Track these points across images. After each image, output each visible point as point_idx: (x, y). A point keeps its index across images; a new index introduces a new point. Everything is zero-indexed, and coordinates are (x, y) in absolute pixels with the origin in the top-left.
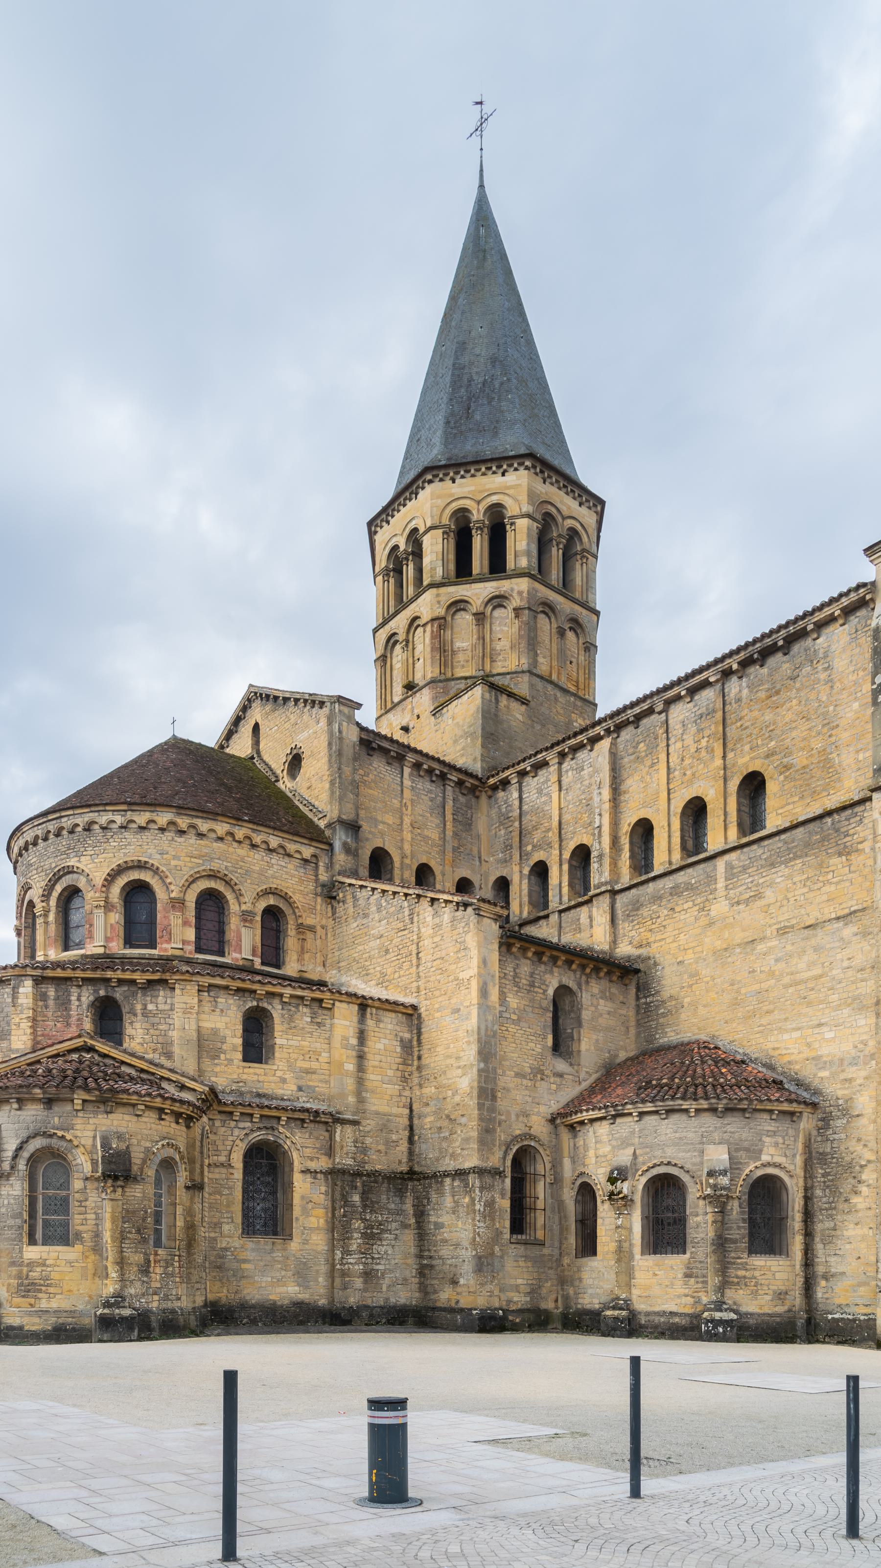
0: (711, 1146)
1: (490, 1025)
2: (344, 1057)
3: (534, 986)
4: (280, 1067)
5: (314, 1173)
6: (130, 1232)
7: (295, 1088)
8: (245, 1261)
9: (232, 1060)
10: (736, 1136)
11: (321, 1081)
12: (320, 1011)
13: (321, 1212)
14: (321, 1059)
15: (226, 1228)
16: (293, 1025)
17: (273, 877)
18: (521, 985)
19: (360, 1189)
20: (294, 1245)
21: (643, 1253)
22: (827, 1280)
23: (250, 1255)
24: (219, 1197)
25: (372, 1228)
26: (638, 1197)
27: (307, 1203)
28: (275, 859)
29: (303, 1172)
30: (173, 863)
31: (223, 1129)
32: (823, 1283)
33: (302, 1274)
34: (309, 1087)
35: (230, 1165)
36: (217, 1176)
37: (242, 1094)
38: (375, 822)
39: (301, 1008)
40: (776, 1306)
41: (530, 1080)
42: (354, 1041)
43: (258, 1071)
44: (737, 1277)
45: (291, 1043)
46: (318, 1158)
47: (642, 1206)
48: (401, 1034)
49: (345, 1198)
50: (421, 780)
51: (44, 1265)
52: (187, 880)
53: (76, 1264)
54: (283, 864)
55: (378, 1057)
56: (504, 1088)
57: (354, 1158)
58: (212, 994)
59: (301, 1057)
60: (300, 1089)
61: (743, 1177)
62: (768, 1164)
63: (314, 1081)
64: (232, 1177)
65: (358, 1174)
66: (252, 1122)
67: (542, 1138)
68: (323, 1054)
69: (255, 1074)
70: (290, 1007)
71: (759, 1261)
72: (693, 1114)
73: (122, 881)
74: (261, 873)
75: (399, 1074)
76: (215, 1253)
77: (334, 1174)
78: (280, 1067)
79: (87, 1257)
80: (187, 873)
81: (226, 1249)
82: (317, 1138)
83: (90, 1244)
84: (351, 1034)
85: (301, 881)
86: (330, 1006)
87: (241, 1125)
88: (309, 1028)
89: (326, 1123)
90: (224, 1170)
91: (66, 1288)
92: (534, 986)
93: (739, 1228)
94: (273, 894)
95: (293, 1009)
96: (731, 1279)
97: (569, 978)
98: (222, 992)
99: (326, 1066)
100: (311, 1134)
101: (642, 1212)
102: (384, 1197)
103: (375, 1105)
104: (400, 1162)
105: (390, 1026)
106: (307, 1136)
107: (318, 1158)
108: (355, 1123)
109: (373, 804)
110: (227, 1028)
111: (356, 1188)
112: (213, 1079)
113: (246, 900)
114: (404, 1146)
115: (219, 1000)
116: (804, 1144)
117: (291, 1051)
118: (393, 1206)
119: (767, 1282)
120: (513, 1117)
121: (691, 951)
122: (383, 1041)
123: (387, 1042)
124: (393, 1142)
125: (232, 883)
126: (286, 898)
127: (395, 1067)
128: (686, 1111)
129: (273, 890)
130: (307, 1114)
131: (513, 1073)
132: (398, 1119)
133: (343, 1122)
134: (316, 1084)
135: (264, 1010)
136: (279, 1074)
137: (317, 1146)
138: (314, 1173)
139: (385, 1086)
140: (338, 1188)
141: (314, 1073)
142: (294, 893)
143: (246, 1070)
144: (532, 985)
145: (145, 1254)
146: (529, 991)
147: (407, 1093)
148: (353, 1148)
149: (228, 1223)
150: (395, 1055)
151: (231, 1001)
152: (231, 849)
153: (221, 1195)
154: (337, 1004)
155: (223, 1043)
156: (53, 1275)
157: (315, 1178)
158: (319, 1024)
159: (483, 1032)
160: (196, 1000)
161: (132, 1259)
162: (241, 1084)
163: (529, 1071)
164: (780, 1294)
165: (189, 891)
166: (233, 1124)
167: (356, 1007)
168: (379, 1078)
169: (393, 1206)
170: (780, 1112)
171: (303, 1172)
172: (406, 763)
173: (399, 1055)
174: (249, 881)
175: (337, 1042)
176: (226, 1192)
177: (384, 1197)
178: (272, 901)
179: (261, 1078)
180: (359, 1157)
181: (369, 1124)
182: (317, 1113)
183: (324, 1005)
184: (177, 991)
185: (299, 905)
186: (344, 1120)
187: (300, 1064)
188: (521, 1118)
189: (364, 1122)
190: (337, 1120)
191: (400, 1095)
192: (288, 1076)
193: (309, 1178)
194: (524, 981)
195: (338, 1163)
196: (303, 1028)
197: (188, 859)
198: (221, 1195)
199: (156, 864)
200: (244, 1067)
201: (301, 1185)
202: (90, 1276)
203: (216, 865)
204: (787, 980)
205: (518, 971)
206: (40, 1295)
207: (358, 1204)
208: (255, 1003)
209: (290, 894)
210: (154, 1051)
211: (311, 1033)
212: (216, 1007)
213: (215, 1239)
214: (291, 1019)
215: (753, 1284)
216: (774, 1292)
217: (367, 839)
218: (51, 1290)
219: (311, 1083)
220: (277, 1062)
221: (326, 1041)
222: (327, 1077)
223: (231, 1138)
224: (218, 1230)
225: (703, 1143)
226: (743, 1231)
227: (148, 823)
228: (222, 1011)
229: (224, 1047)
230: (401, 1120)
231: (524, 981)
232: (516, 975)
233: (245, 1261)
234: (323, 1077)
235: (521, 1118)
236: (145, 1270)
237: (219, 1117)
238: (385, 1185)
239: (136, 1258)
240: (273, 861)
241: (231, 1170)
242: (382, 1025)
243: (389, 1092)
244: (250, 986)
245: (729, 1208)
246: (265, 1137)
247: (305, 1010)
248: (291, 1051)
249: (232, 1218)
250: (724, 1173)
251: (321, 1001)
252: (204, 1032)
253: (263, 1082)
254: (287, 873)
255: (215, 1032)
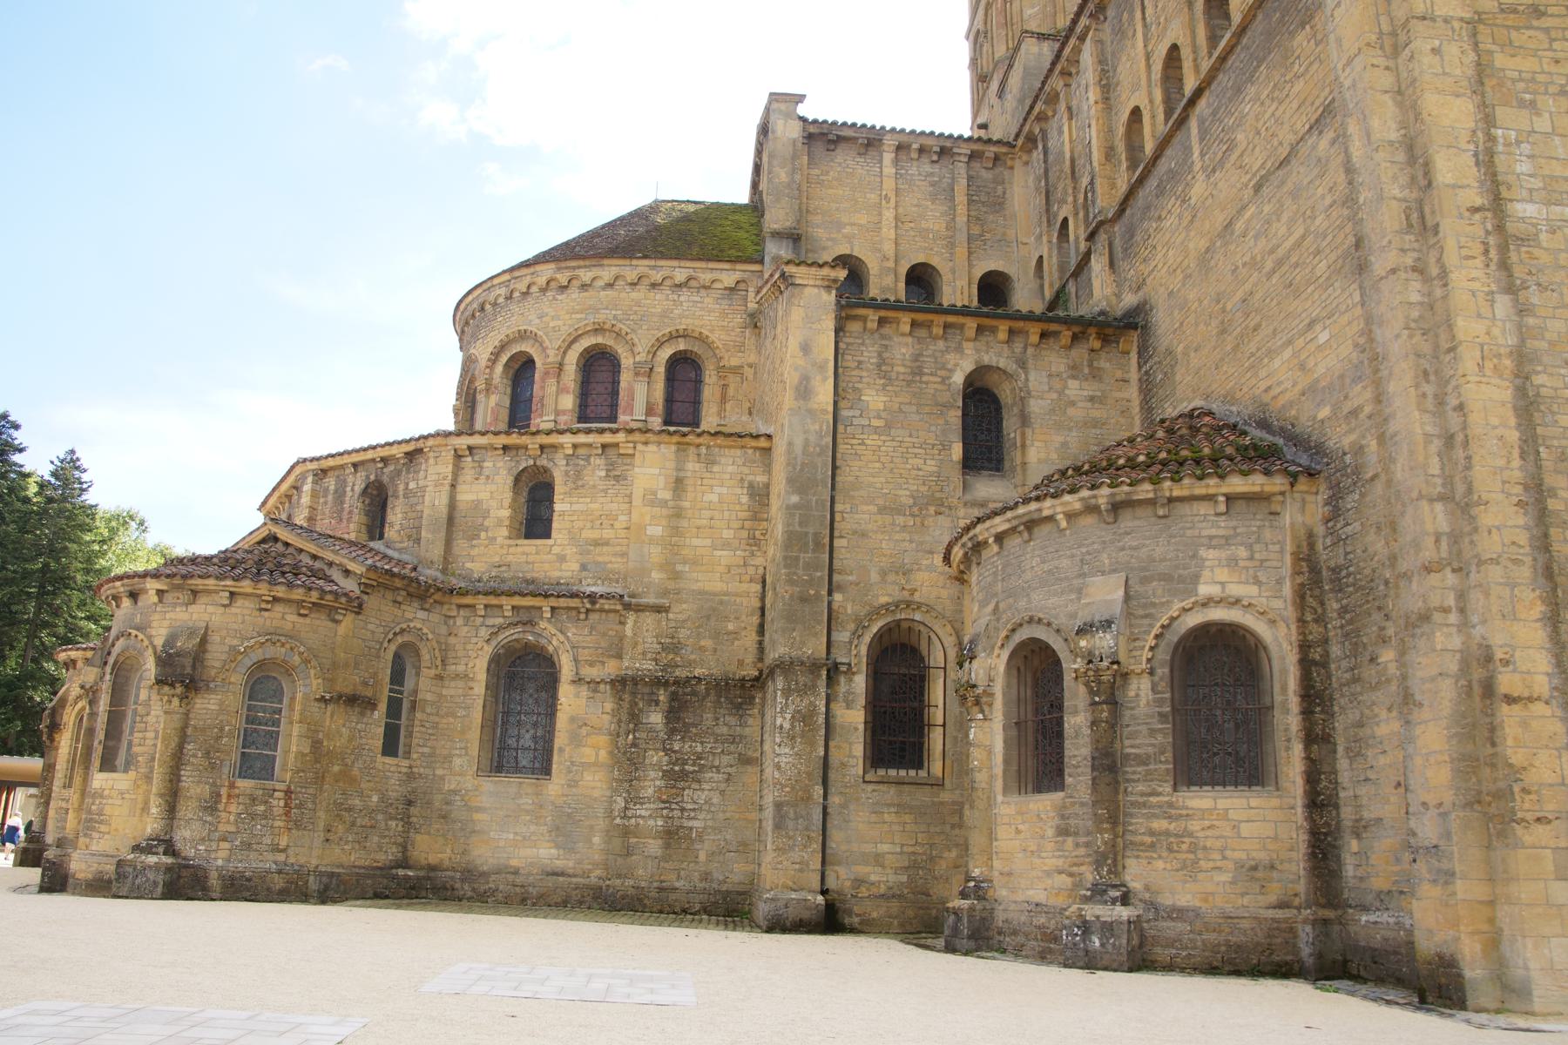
0: (1098, 579)
1: (812, 438)
2: (648, 518)
3: (921, 374)
4: (559, 541)
5: (594, 684)
6: (195, 756)
7: (575, 566)
8: (479, 810)
9: (495, 538)
10: (1143, 553)
11: (615, 555)
12: (620, 461)
13: (603, 740)
14: (617, 525)
15: (457, 762)
16: (580, 483)
17: (681, 317)
18: (894, 375)
19: (664, 705)
20: (554, 787)
21: (1006, 791)
22: (1358, 836)
23: (485, 801)
24: (451, 720)
25: (685, 763)
26: (998, 689)
27: (580, 727)
28: (685, 296)
29: (574, 682)
30: (551, 325)
31: (466, 629)
32: (1354, 845)
33: (564, 828)
34: (597, 563)
35: (466, 676)
36: (452, 692)
37: (503, 581)
38: (840, 226)
39: (592, 459)
40: (1243, 895)
41: (913, 515)
42: (666, 495)
43: (526, 549)
44: (1152, 833)
45: (575, 507)
46: (603, 663)
47: (1005, 704)
48: (751, 478)
49: (635, 718)
50: (915, 163)
51: (102, 797)
52: (564, 341)
53: (127, 796)
54: (698, 299)
55: (707, 514)
56: (855, 532)
57: (656, 660)
58: (476, 458)
59: (589, 525)
60: (584, 567)
61: (1156, 630)
62: (1207, 603)
63: (604, 556)
64: (470, 692)
65: (659, 682)
66: (504, 617)
67: (939, 608)
68: (622, 518)
69: (524, 553)
70: (577, 461)
71: (1199, 800)
72: (1064, 524)
73: (504, 358)
74: (664, 314)
75: (745, 534)
76: (440, 797)
77: (621, 684)
78: (559, 541)
79: (138, 787)
80: (565, 331)
81: (455, 792)
82: (604, 635)
83: (142, 770)
84: (661, 485)
85: (724, 315)
86: (630, 452)
87: (490, 622)
88: (602, 485)
89: (618, 611)
90: (460, 684)
91: (114, 826)
92: (921, 374)
93: (1152, 732)
94: (684, 336)
95: (582, 462)
96: (1138, 839)
97: (1000, 355)
98: (489, 454)
99: (623, 533)
100: (592, 628)
101: (1006, 715)
102: (709, 716)
103: (697, 581)
104: (741, 663)
105: (730, 469)
106: (586, 631)
107: (603, 663)
108: (659, 609)
109: (834, 206)
110: (492, 498)
111: (657, 703)
112: (468, 565)
113: (640, 349)
114: (750, 638)
115: (486, 464)
116: (1297, 558)
117: (575, 518)
118: (725, 730)
119: (1218, 844)
120: (874, 577)
121: (1179, 271)
122: (717, 490)
123: (724, 490)
124: (728, 633)
125: (623, 333)
126: (701, 339)
127: (736, 525)
128: (1051, 519)
129: (681, 333)
130: (576, 600)
131: (873, 509)
132: (738, 600)
133: (639, 609)
134: (606, 559)
135: (546, 470)
136: (556, 550)
137: (603, 645)
138: (594, 684)
139: (719, 553)
140: (626, 705)
141: (607, 544)
142: (712, 331)
143: (512, 550)
144: (918, 372)
145: (214, 784)
146: (909, 383)
147: (759, 561)
148: (655, 646)
149: (460, 756)
150: (738, 507)
151: (500, 464)
152: (623, 295)
153: (454, 715)
154: (640, 447)
155: (485, 518)
156: (107, 810)
157: (595, 691)
158: (617, 479)
159: (798, 449)
160: (450, 468)
161: (192, 791)
162: (503, 569)
163: (911, 501)
164: (1255, 868)
165: (570, 352)
166: (479, 620)
167: (673, 448)
168: (708, 542)
169: (725, 730)
170: (1230, 499)
171: (574, 682)
172: (885, 148)
173: (746, 507)
174: (645, 327)
175: (637, 501)
176: (461, 713)
177: (709, 716)
178: (682, 345)
179: (531, 558)
180: (666, 658)
181: (682, 610)
182: (592, 598)
183: (621, 451)
184: (431, 461)
185: (718, 344)
186: (638, 605)
187: (588, 534)
188: (891, 578)
189: (675, 609)
190: (629, 605)
191: (745, 565)
192: (570, 551)
193: (584, 691)
194: (902, 369)
195: (627, 668)
196: (594, 486)
197: (567, 317)
198: (454, 715)
199: (535, 330)
200: (510, 546)
201: (569, 699)
202: (138, 812)
203: (601, 317)
204: (1269, 265)
205: (886, 355)
206: (95, 835)
207: (660, 727)
208: (531, 462)
209: (706, 332)
210: (409, 537)
211: (605, 492)
212: (480, 474)
213: (442, 778)
214: (578, 475)
215: (1184, 847)
216: (1240, 865)
217: (824, 248)
218: (103, 828)
219: (600, 559)
220: (554, 534)
221: (627, 499)
222: (624, 548)
223: (474, 640)
224: (446, 765)
225: (1083, 575)
226: (1160, 737)
227: (529, 287)
228: (488, 477)
229: (486, 523)
230: (745, 601)
231: (902, 369)
232: (882, 362)
233: (479, 810)
234: (618, 548)
235: (891, 578)
236: (211, 806)
237: (462, 612)
238: (712, 697)
239: (199, 790)
240: (682, 298)
241: (471, 684)
242: (716, 468)
243: (723, 562)
244: (518, 441)
245: (1132, 694)
246: (521, 636)
247: (598, 461)
248: (575, 518)
249: (466, 748)
250: (1107, 624)
251: (616, 445)
252: (461, 506)
253: (533, 563)
254: (702, 309)
255: (477, 504)
